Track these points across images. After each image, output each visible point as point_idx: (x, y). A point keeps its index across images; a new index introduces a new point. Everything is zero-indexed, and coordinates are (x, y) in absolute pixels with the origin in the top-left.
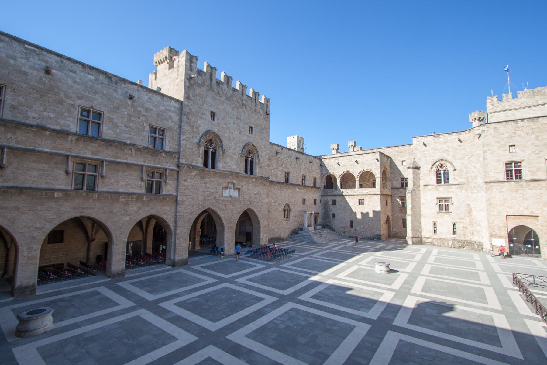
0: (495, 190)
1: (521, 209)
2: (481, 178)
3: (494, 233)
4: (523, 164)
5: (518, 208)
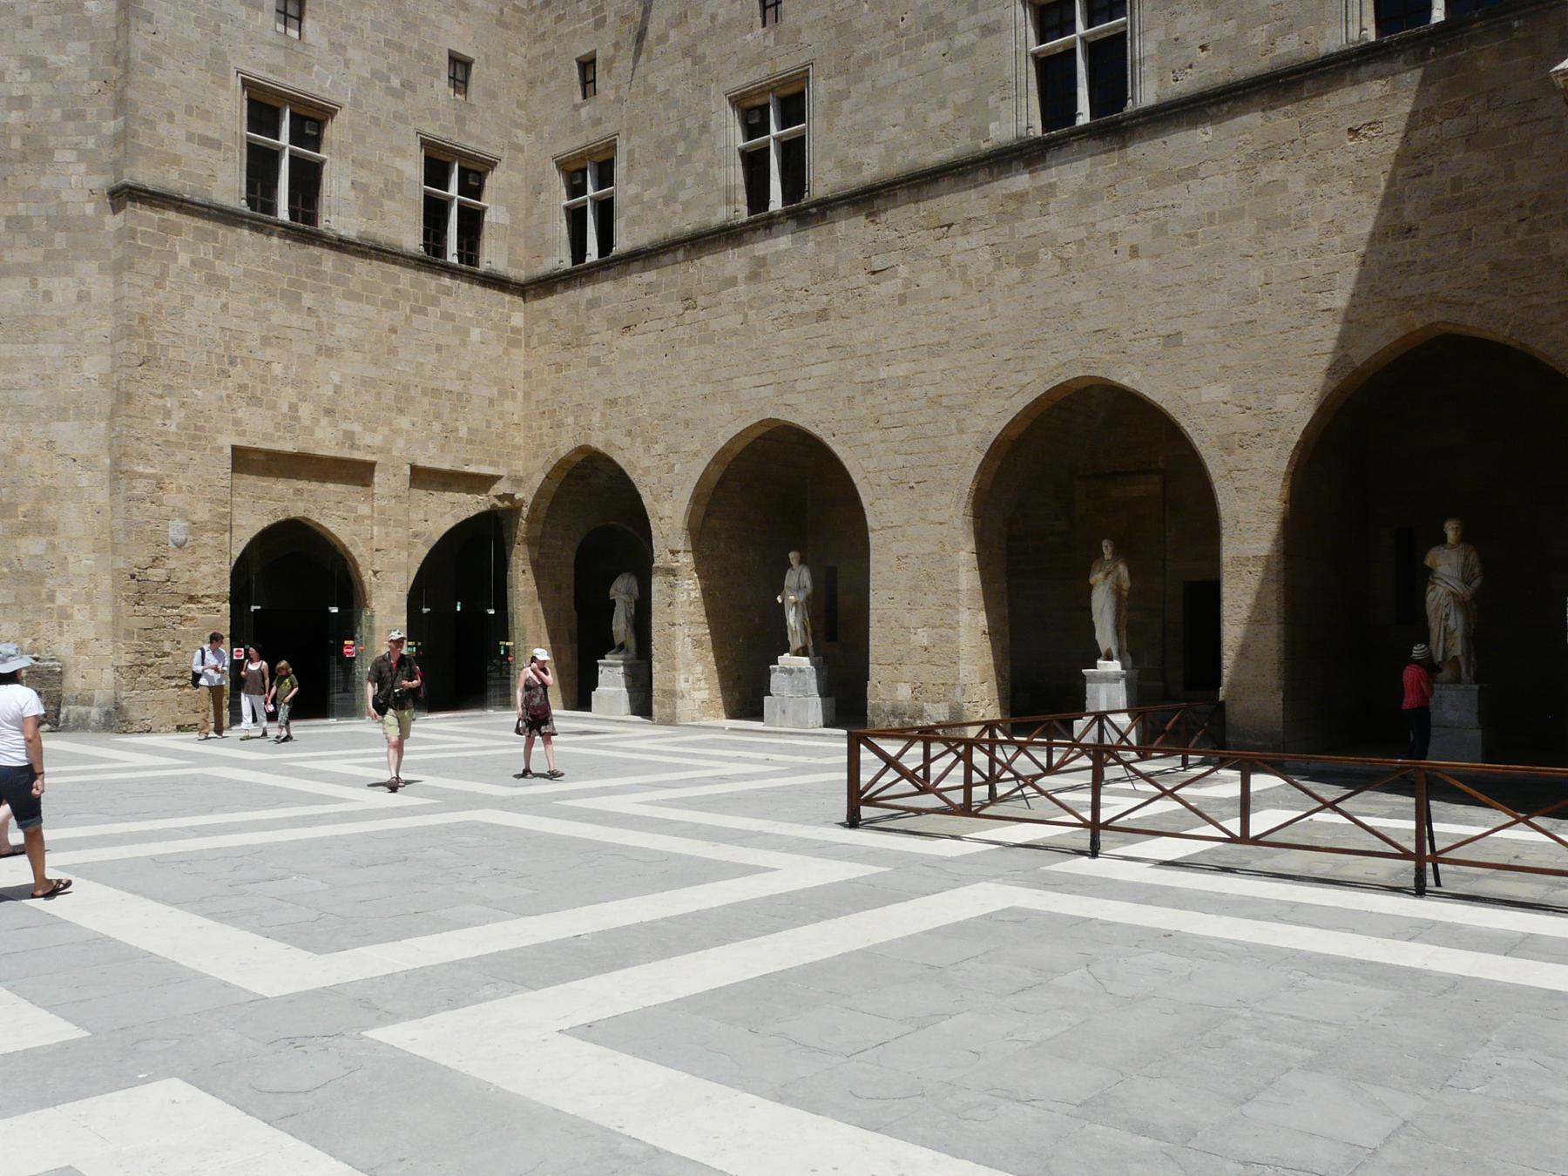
0: (184, 259)
1: (305, 410)
2: (83, 156)
3: (157, 574)
4: (332, 132)
5: (293, 407)
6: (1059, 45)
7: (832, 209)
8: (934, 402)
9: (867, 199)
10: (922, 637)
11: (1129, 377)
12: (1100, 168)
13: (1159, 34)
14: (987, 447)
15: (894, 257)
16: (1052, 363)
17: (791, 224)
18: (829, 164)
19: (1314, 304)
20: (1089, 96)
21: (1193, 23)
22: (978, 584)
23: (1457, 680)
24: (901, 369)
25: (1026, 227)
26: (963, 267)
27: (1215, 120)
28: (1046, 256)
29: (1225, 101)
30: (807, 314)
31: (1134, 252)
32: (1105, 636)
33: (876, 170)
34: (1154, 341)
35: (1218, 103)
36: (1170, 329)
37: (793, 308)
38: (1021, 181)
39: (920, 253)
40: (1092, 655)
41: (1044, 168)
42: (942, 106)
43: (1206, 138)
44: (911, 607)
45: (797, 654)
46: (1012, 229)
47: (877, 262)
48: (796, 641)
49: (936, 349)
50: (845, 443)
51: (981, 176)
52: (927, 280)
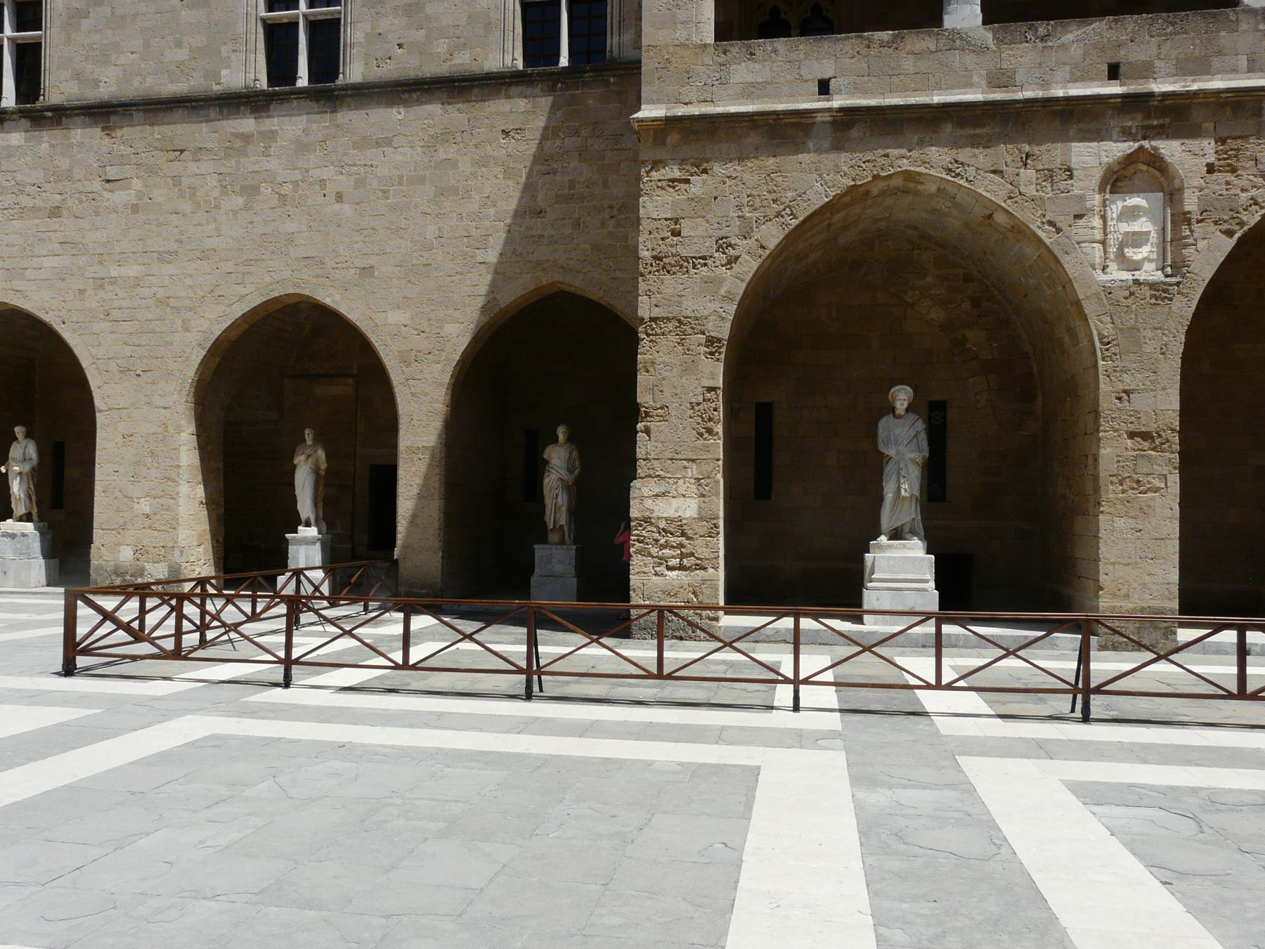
6: (285, 17)
7: (68, 116)
8: (162, 302)
9: (104, 113)
10: (145, 506)
11: (330, 298)
12: (315, 126)
13: (366, 27)
14: (208, 345)
15: (128, 171)
16: (268, 279)
17: (25, 123)
18: (66, 74)
19: (473, 257)
20: (305, 63)
21: (392, 24)
22: (197, 462)
23: (562, 542)
24: (133, 271)
25: (252, 162)
26: (193, 189)
27: (407, 104)
28: (266, 189)
29: (415, 91)
30: (40, 209)
31: (339, 197)
32: (305, 506)
33: (113, 89)
34: (353, 271)
35: (409, 91)
36: (365, 262)
37: (25, 201)
38: (247, 124)
39: (153, 171)
40: (293, 522)
41: (268, 117)
42: (179, 45)
43: (400, 117)
44: (135, 479)
45: (20, 520)
46: (238, 162)
47: (112, 173)
48: (19, 508)
49: (165, 257)
50: (74, 331)
51: (212, 113)
52: (159, 195)
